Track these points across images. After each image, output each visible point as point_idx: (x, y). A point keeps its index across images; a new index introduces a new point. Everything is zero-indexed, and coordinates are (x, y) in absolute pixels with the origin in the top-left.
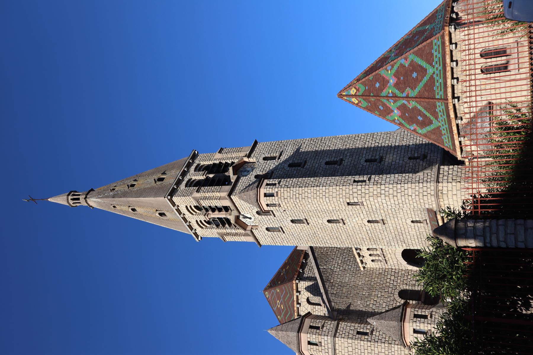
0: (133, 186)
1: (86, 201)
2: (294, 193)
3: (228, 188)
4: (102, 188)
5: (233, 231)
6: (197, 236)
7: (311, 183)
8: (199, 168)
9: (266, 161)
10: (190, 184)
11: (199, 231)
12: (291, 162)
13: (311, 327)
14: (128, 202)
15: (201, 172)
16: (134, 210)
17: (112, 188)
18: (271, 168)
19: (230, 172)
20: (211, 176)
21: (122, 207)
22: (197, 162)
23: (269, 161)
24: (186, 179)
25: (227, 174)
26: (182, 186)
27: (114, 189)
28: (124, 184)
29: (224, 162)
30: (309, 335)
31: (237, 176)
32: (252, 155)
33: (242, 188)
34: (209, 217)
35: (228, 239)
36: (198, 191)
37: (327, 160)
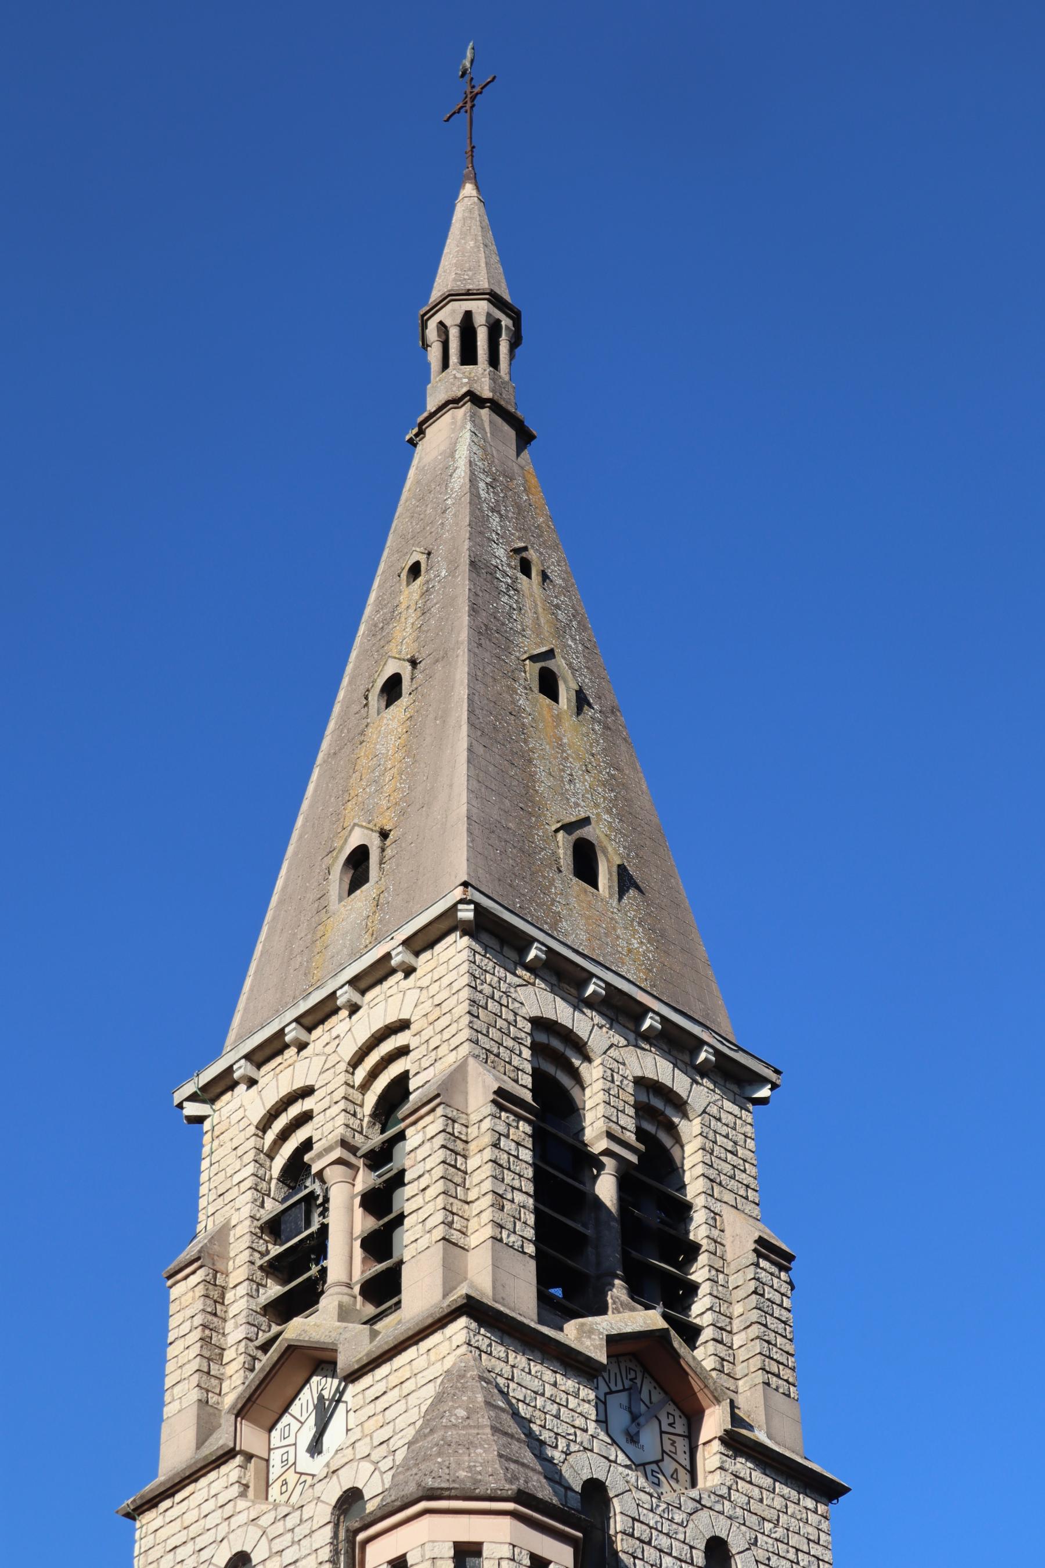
0: (548, 685)
1: (454, 402)
3: (522, 1301)
4: (537, 497)
5: (235, 1333)
6: (210, 1093)
8: (656, 1106)
10: (555, 1052)
11: (243, 1107)
14: (444, 657)
15: (630, 1123)
16: (392, 689)
17: (532, 555)
19: (629, 1317)
20: (606, 1188)
21: (412, 617)
22: (701, 1095)
24: (584, 1024)
25: (618, 1291)
26: (539, 1000)
27: (525, 568)
28: (560, 631)
29: (699, 1273)
32: (742, 1466)
33: (516, 1393)
34: (334, 1174)
35: (186, 1296)
36: (503, 1099)
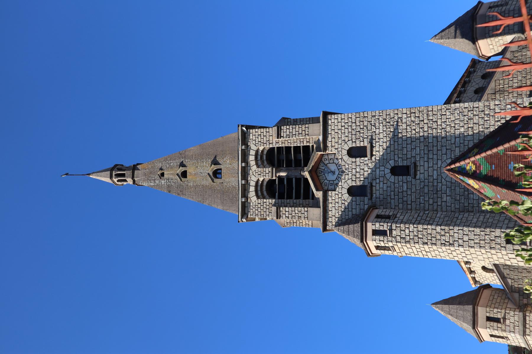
2: (418, 250)
7: (438, 237)
9: (354, 160)
12: (392, 163)
13: (489, 319)
17: (159, 173)
18: (366, 174)
22: (253, 147)
23: (358, 159)
30: (488, 330)
31: (321, 192)
32: (329, 144)
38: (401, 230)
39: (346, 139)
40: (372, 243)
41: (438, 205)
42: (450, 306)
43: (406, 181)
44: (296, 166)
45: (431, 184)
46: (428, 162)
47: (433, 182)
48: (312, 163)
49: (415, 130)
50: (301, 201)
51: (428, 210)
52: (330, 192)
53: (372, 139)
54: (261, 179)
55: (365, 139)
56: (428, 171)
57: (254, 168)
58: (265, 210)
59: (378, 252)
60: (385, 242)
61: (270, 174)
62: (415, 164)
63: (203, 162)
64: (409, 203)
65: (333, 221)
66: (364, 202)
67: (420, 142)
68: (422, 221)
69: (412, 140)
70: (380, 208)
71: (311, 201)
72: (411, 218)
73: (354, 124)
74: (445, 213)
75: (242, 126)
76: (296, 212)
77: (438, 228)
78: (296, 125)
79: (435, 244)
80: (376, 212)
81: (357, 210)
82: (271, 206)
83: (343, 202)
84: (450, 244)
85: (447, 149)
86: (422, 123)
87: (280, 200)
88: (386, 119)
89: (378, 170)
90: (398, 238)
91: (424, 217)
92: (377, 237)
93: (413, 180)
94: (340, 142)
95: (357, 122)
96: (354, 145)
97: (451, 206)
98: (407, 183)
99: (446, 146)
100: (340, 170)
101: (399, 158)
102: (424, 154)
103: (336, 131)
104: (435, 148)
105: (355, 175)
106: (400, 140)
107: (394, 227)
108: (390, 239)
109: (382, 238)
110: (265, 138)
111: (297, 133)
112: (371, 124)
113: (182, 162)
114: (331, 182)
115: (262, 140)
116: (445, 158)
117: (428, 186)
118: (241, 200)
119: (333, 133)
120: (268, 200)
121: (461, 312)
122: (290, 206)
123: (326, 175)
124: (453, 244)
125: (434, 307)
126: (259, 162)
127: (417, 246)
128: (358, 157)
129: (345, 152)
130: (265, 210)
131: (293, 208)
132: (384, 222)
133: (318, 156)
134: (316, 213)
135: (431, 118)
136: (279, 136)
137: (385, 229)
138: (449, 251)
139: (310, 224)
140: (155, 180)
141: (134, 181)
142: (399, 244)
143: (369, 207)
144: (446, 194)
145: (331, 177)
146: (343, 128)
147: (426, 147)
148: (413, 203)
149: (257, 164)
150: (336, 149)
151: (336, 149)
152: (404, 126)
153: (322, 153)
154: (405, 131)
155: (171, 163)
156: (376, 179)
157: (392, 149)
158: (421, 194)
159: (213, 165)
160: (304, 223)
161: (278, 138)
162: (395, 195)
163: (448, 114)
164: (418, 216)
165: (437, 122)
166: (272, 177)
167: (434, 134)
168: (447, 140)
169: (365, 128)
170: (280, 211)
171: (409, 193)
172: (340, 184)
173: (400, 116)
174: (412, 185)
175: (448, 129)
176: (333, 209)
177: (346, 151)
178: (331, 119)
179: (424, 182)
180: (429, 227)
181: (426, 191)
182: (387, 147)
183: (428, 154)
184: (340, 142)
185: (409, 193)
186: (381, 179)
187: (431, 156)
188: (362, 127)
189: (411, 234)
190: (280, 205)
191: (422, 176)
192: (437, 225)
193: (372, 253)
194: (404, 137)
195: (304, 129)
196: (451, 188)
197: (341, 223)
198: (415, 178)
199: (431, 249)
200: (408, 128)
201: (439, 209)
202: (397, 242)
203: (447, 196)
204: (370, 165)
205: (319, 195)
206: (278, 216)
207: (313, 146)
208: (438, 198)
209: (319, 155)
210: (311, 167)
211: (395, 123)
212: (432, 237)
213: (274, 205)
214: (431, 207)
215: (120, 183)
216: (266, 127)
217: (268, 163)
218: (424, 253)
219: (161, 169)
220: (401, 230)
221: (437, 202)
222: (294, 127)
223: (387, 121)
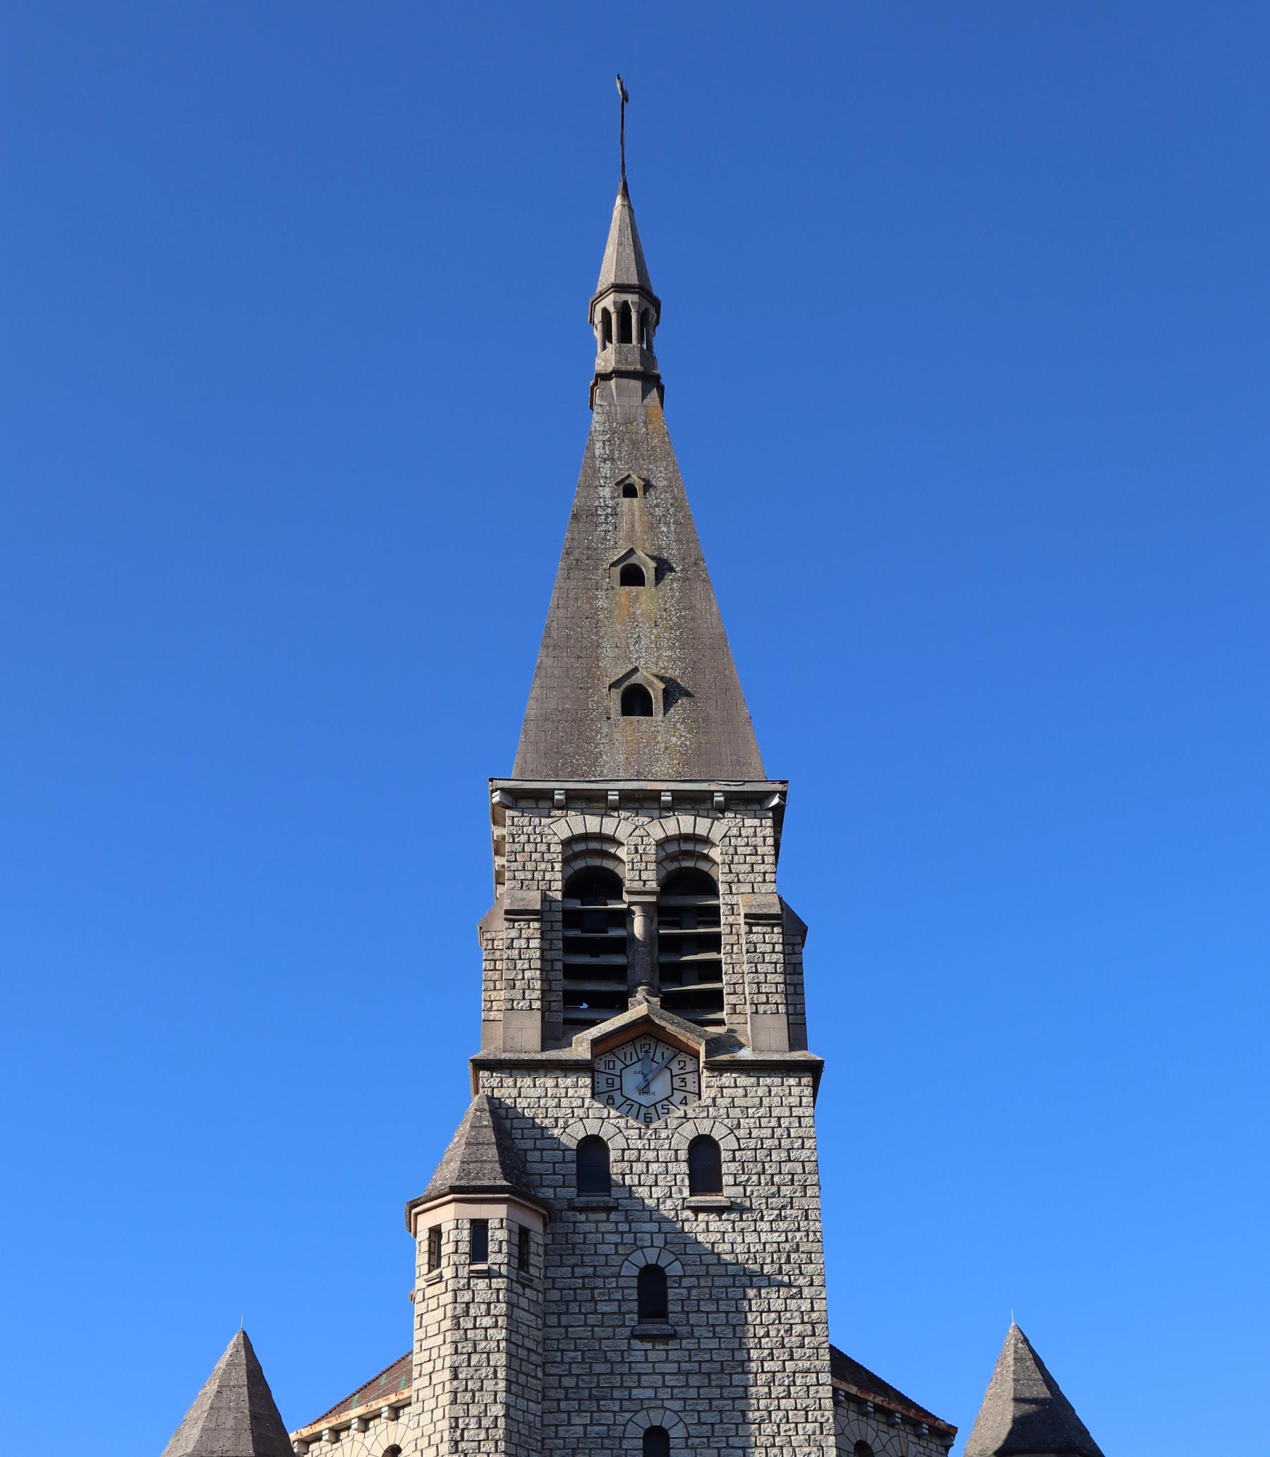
2: (435, 1351)
7: (474, 1410)
9: (683, 1155)
12: (675, 1269)
18: (642, 1192)
22: (718, 829)
23: (684, 1167)
31: (588, 1056)
32: (727, 1079)
37: (677, 1433)
38: (489, 1304)
39: (742, 1133)
40: (447, 1216)
41: (559, 1400)
42: (245, 1390)
43: (623, 1310)
44: (663, 966)
45: (617, 1381)
46: (679, 1373)
47: (622, 1386)
48: (672, 1024)
49: (767, 1335)
50: (560, 985)
51: (544, 1374)
52: (588, 1081)
53: (741, 1210)
54: (622, 853)
55: (741, 1189)
56: (654, 1373)
57: (657, 832)
58: (530, 866)
59: (423, 1235)
60: (454, 1258)
61: (637, 886)
62: (673, 1336)
63: (672, 648)
64: (564, 1319)
65: (505, 1092)
66: (563, 1186)
67: (733, 1350)
68: (516, 1364)
69: (738, 1327)
70: (546, 1233)
71: (560, 1018)
72: (523, 1330)
73: (784, 1155)
74: (539, 1425)
75: (783, 794)
76: (528, 974)
77: (498, 1410)
78: (785, 973)
79: (454, 1402)
80: (535, 1225)
81: (540, 1166)
82: (543, 886)
83: (561, 1122)
84: (457, 1443)
85: (713, 1424)
86: (786, 1357)
87: (559, 916)
88: (797, 1250)
89: (653, 1227)
90: (467, 1296)
91: (527, 1368)
92: (466, 1235)
93: (627, 1332)
94: (735, 1113)
95: (789, 1164)
96: (725, 1156)
97: (556, 1437)
98: (619, 1313)
99: (721, 1422)
100: (652, 1110)
101: (689, 1289)
102: (700, 1362)
103: (766, 1101)
104: (716, 1392)
105: (638, 1160)
106: (738, 1293)
107: (497, 1283)
108: (464, 1272)
109: (465, 1247)
110: (747, 868)
111: (762, 978)
112: (784, 1207)
113: (672, 570)
114: (617, 1080)
115: (736, 851)
116: (688, 1420)
117: (612, 1373)
118: (559, 787)
119: (761, 1091)
120: (559, 876)
121: (231, 1423)
122: (542, 950)
123: (638, 1067)
124: (457, 1451)
125: (236, 1338)
126: (672, 848)
127: (447, 1349)
128: (690, 1167)
129: (704, 1127)
130: (530, 866)
131: (538, 964)
132: (509, 1255)
133: (691, 1043)
134: (526, 1037)
135: (798, 1382)
136: (754, 919)
137: (492, 1258)
138: (436, 1439)
139: (493, 1015)
140: (612, 460)
141: (605, 377)
142: (448, 1297)
143: (549, 1199)
144: (592, 1424)
145: (631, 1081)
146: (774, 1123)
147: (718, 1366)
148: (562, 1330)
149: (668, 839)
150: (714, 1099)
151: (714, 1099)
152: (777, 1305)
153: (702, 1058)
154: (765, 1306)
155: (667, 524)
156: (627, 1221)
157: (713, 1270)
158: (589, 1354)
159: (662, 686)
160: (494, 995)
161: (746, 916)
162: (583, 1278)
163: (810, 1427)
164: (529, 1350)
165: (788, 1396)
166: (629, 893)
167: (753, 1390)
168: (737, 1424)
169: (774, 1189)
170: (529, 921)
171: (592, 1319)
172: (613, 1113)
173: (806, 1291)
174: (614, 1327)
175: (768, 1428)
176: (540, 1092)
177: (707, 1132)
178: (799, 1084)
179: (623, 1361)
180: (502, 1385)
181: (598, 1368)
182: (719, 1254)
183: (700, 1372)
184: (733, 1113)
185: (592, 1319)
186: (629, 1238)
187: (694, 1380)
188: (776, 1179)
189: (480, 1333)
190: (547, 916)
191: (639, 1356)
192: (508, 1406)
193: (417, 1214)
194: (746, 1303)
195: (772, 999)
196: (608, 1437)
197: (500, 1115)
198: (634, 1336)
199: (439, 1389)
200: (773, 1315)
201: (547, 1404)
202: (454, 1291)
203: (585, 1426)
204: (669, 1202)
205: (580, 1047)
206: (513, 915)
207: (721, 1022)
208: (580, 1400)
209: (696, 1046)
210: (663, 1023)
211: (786, 1279)
212: (473, 1391)
213: (545, 899)
214: (553, 1381)
215: (598, 317)
216: (776, 855)
217: (670, 874)
218: (428, 1368)
219: (648, 486)
220: (489, 1304)
221: (567, 1398)
222: (780, 968)
223: (793, 1256)
